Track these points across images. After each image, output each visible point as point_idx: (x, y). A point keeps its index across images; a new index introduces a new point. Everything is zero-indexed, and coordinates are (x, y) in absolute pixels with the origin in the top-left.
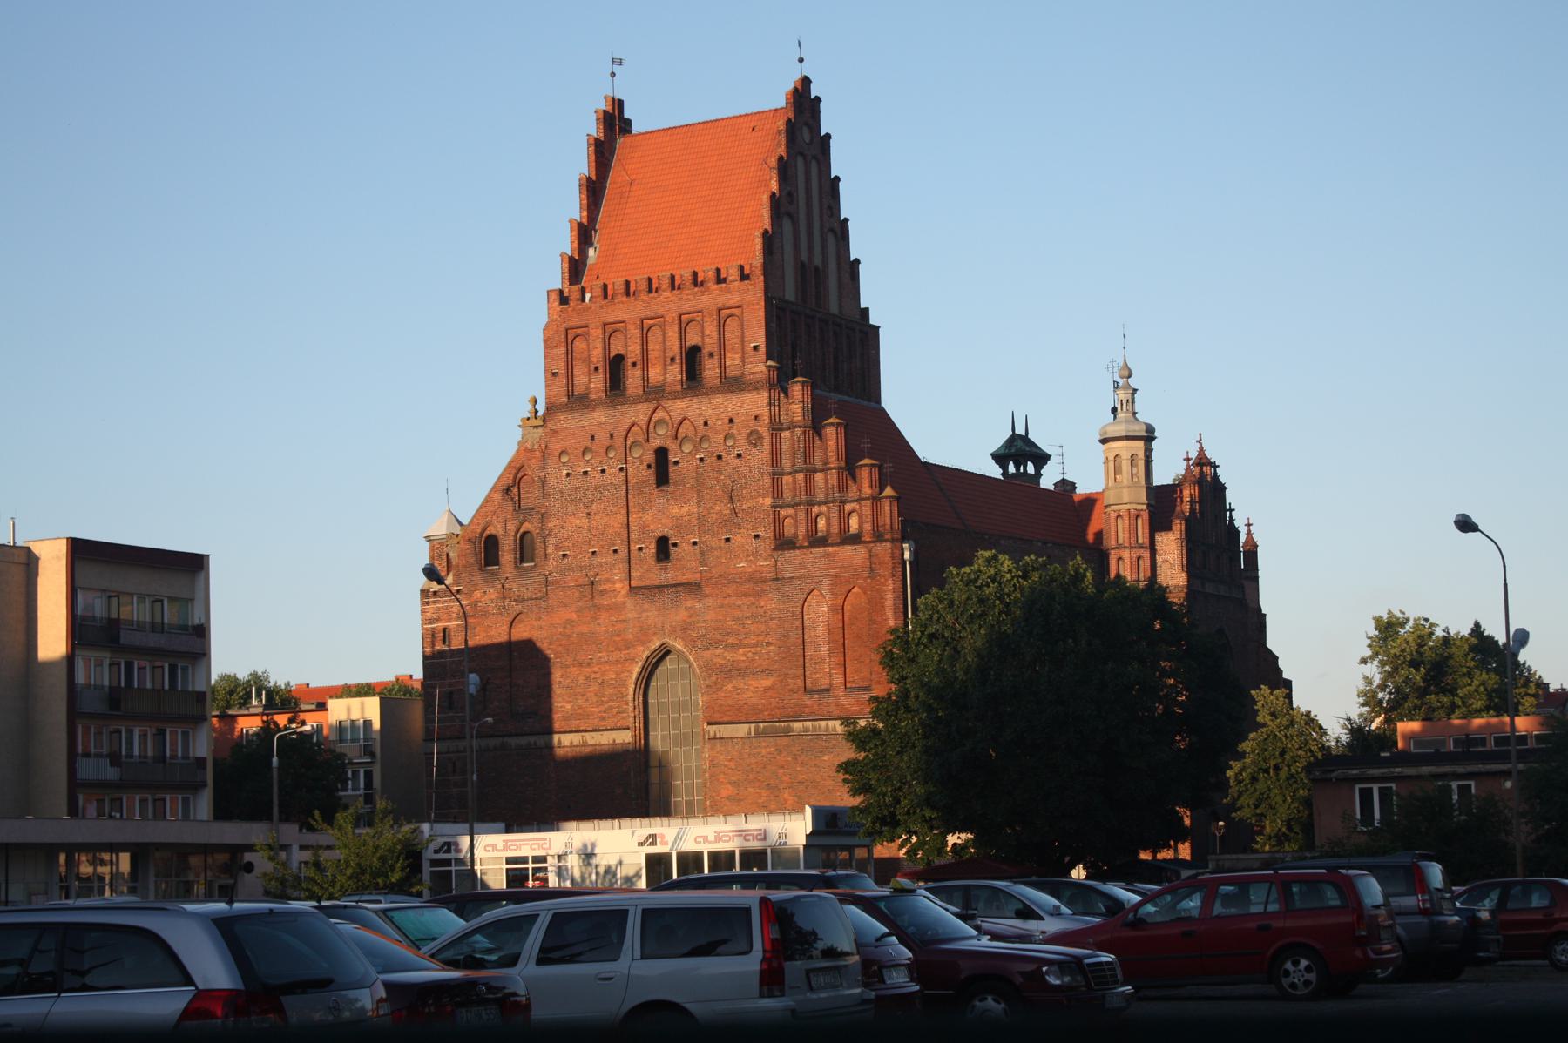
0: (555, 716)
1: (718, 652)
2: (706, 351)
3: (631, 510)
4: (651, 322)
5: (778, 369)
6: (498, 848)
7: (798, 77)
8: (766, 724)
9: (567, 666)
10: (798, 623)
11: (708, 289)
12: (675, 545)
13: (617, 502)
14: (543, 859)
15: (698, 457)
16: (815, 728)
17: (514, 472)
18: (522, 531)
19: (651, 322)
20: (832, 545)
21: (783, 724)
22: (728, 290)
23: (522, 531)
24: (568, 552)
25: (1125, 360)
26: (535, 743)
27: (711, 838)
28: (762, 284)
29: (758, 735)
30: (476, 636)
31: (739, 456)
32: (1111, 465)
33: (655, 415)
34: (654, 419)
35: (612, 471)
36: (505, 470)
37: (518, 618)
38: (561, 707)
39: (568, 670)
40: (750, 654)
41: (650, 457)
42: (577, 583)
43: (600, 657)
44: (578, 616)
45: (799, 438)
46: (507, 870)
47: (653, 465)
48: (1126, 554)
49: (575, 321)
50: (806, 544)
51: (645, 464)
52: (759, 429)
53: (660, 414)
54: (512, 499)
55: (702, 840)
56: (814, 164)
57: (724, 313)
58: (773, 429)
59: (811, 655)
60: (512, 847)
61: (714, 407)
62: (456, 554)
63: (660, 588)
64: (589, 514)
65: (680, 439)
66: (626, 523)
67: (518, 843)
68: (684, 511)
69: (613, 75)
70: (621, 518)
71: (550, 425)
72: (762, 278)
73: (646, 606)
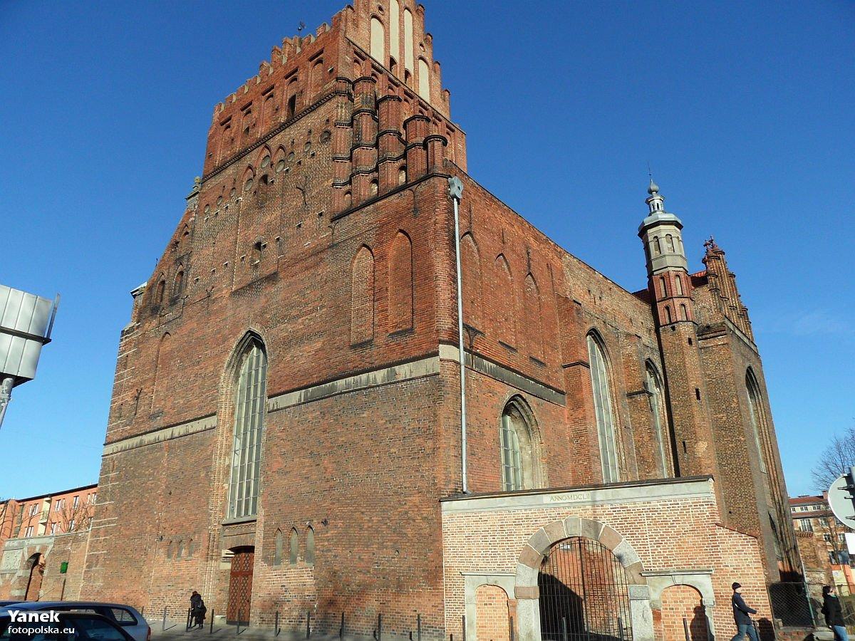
16: (356, 383)
21: (328, 384)
40: (307, 321)
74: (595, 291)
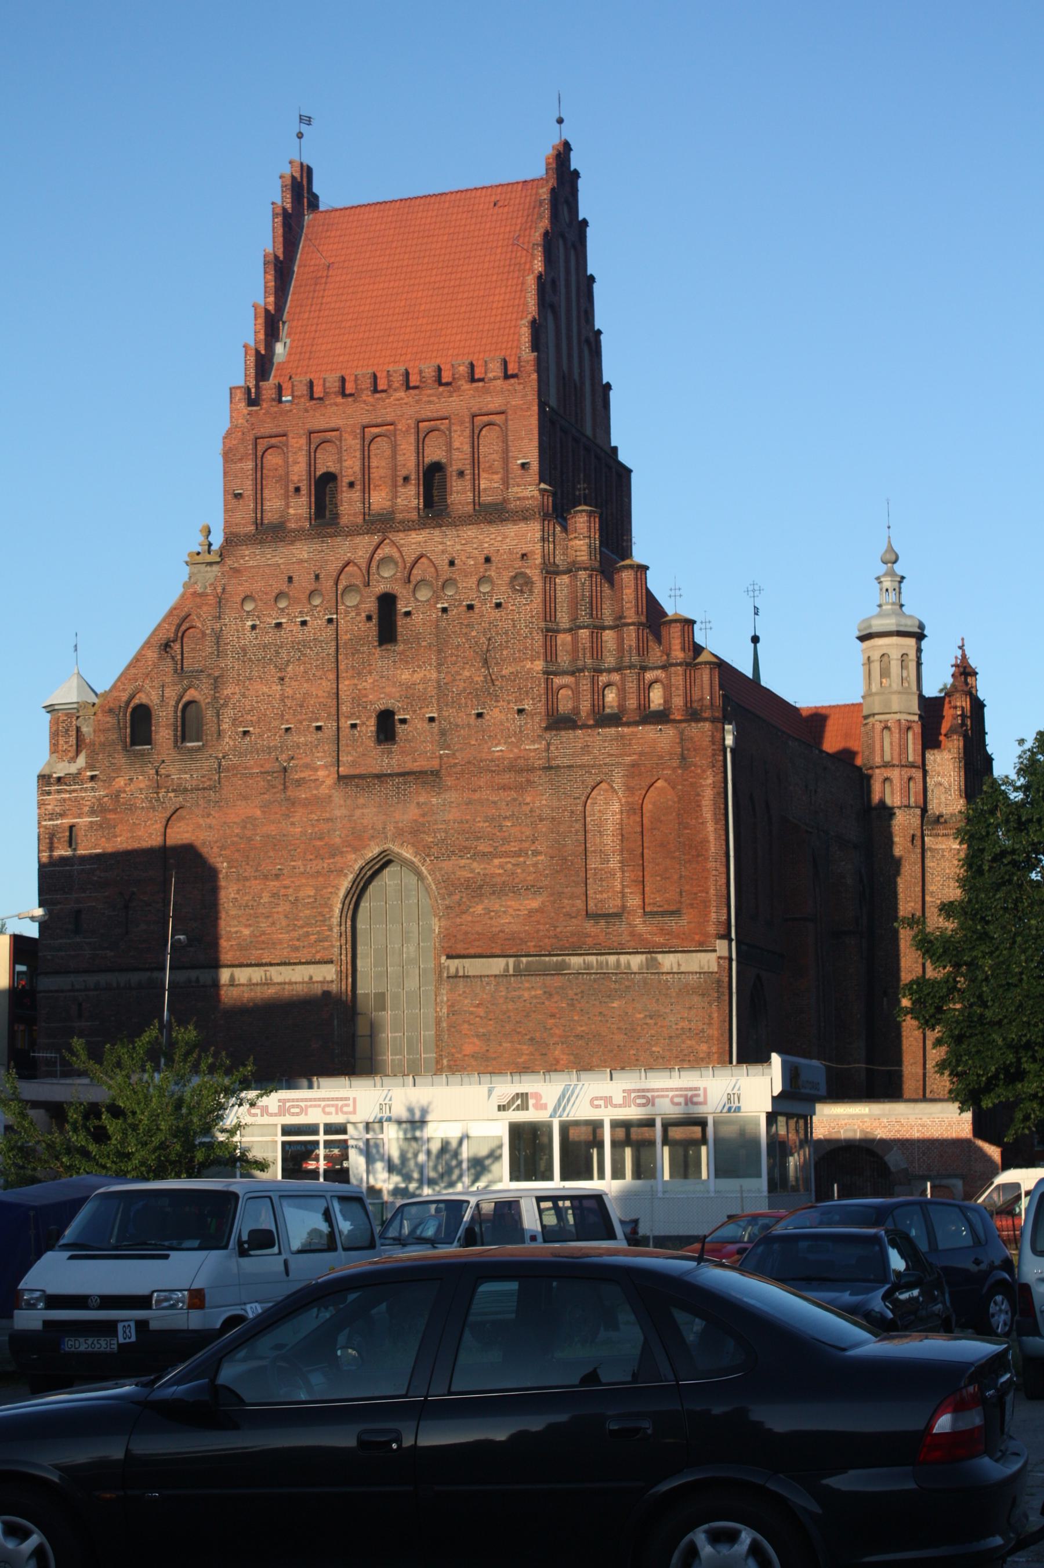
0: (223, 943)
1: (463, 862)
2: (453, 469)
3: (342, 674)
4: (376, 430)
5: (554, 494)
6: (270, 1111)
7: (556, 141)
8: (530, 959)
9: (246, 879)
10: (579, 826)
11: (459, 388)
12: (403, 721)
13: (323, 664)
14: (342, 1129)
15: (439, 606)
16: (600, 965)
17: (176, 621)
18: (185, 700)
19: (376, 430)
20: (628, 724)
21: (555, 959)
22: (486, 391)
24: (251, 729)
25: (889, 542)
26: (197, 980)
27: (618, 1099)
28: (535, 385)
29: (518, 973)
30: (116, 836)
31: (498, 605)
32: (876, 667)
33: (379, 551)
34: (377, 557)
35: (316, 623)
36: (164, 620)
37: (177, 814)
38: (236, 932)
39: (247, 884)
40: (510, 866)
41: (371, 605)
42: (263, 770)
43: (294, 868)
44: (264, 812)
45: (583, 584)
46: (284, 1143)
47: (375, 617)
48: (895, 774)
49: (268, 428)
50: (591, 722)
51: (364, 615)
52: (528, 571)
53: (386, 550)
54: (173, 658)
55: (602, 1102)
56: (572, 252)
57: (480, 420)
58: (547, 572)
59: (595, 869)
60: (293, 1110)
61: (463, 542)
62: (91, 729)
63: (380, 777)
64: (282, 679)
65: (414, 582)
66: (335, 691)
67: (302, 1104)
68: (417, 677)
69: (300, 135)
71: (229, 562)
72: (535, 376)
73: (361, 801)
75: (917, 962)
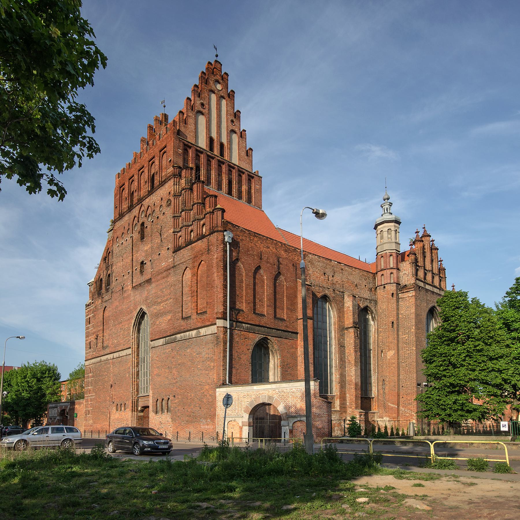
10: (180, 285)
18: (108, 273)
23: (108, 273)
59: (185, 300)
70: (130, 258)
74: (329, 272)
75: (394, 339)
